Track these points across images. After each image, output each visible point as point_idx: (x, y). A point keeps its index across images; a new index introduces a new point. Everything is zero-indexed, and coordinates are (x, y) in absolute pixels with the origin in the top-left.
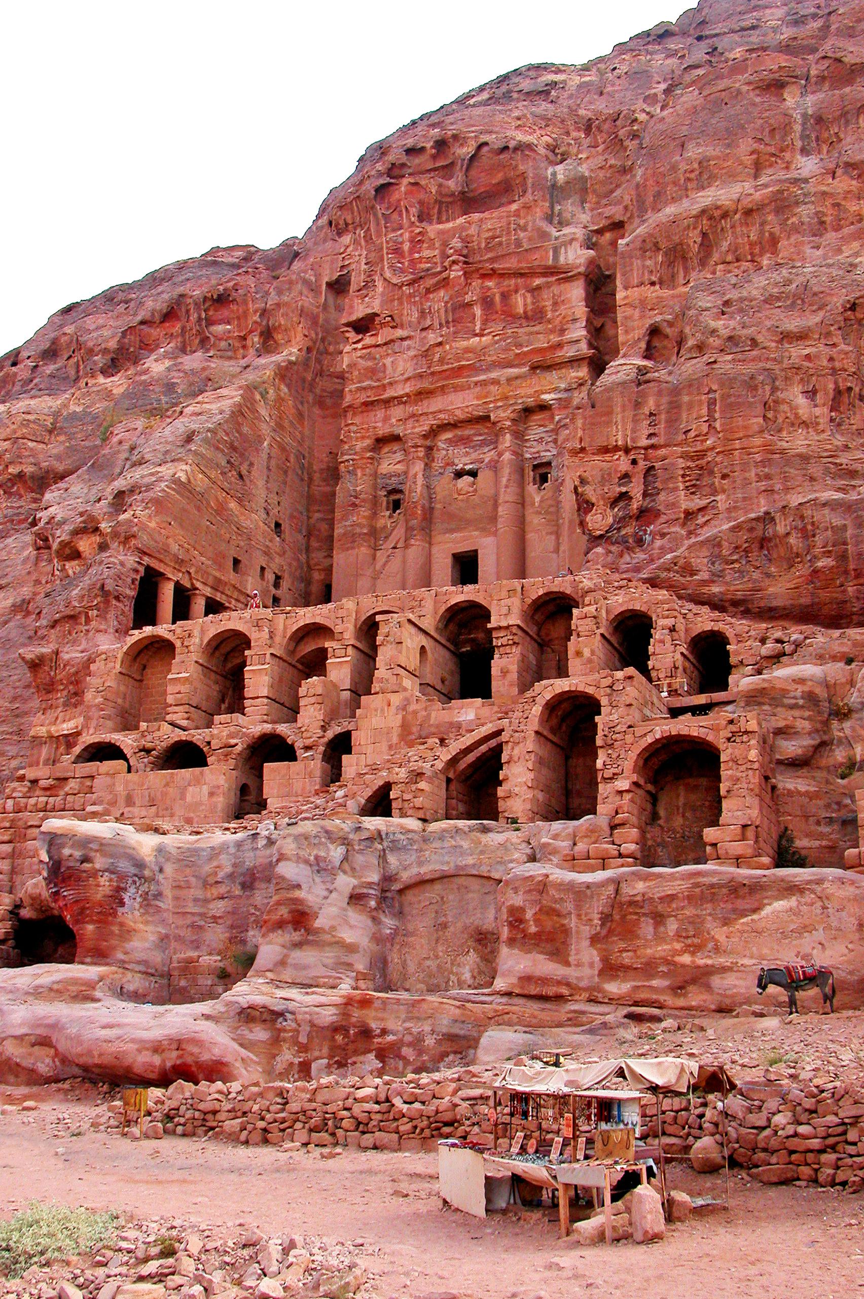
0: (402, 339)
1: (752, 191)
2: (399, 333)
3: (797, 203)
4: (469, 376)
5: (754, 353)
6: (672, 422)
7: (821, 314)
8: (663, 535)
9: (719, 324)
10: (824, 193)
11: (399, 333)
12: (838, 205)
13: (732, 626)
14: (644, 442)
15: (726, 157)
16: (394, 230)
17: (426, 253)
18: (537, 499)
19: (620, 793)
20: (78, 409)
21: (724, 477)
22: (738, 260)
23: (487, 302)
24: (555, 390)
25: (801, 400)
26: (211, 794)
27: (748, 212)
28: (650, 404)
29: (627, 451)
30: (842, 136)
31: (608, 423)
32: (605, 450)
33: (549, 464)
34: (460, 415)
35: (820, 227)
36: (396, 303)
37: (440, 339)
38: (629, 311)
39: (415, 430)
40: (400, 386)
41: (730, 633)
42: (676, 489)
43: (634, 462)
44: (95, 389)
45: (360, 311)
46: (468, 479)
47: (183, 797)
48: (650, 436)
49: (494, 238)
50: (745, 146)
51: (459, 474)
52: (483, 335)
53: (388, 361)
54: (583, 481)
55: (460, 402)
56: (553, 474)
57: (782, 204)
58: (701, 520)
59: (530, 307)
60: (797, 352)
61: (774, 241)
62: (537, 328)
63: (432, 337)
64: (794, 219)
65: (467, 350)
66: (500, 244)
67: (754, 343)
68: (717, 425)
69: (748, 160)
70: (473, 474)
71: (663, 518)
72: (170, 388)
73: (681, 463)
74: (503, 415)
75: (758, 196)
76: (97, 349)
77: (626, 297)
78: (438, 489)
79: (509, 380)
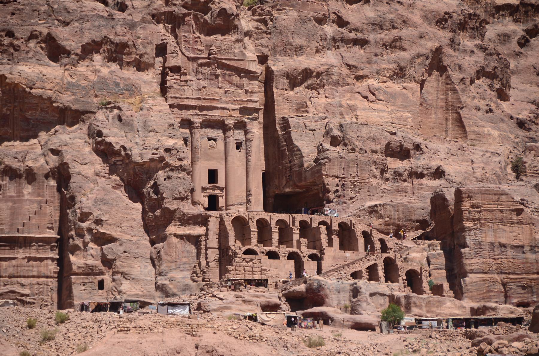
0: (191, 81)
1: (320, 66)
2: (189, 77)
3: (333, 74)
4: (217, 104)
5: (366, 155)
6: (348, 171)
7: (379, 145)
8: (345, 203)
9: (357, 143)
10: (341, 74)
11: (189, 77)
12: (344, 78)
13: (386, 238)
14: (342, 176)
15: (308, 46)
16: (185, 32)
17: (200, 48)
18: (238, 155)
19: (403, 280)
20: (74, 81)
21: (360, 189)
22: (312, 89)
23: (224, 75)
24: (248, 118)
25: (375, 170)
26: (292, 267)
27: (319, 75)
28: (343, 166)
29: (337, 177)
30: (340, 47)
31: (333, 169)
32: (332, 176)
33: (241, 143)
34: (215, 118)
35: (337, 84)
36: (187, 64)
37: (206, 85)
38: (279, 98)
39: (197, 120)
40: (190, 100)
41: (385, 239)
42: (348, 191)
43: (339, 181)
44: (79, 73)
45: (172, 62)
46: (212, 142)
47: (284, 266)
48: (343, 174)
49: (225, 50)
50: (314, 44)
51: (209, 139)
52: (220, 88)
53: (186, 88)
54: (328, 185)
55: (216, 114)
56: (243, 147)
57: (328, 72)
58: (353, 200)
59: (238, 82)
60: (375, 156)
61: (324, 86)
62: (240, 91)
63: (203, 83)
64: (331, 80)
65: (216, 92)
66: (228, 53)
67: (366, 152)
68: (359, 174)
69: (315, 50)
70: (215, 140)
71: (345, 198)
72: (117, 85)
73: (350, 183)
74: (230, 122)
75: (323, 68)
76: (72, 52)
77: (277, 92)
78: (202, 143)
79: (233, 110)
